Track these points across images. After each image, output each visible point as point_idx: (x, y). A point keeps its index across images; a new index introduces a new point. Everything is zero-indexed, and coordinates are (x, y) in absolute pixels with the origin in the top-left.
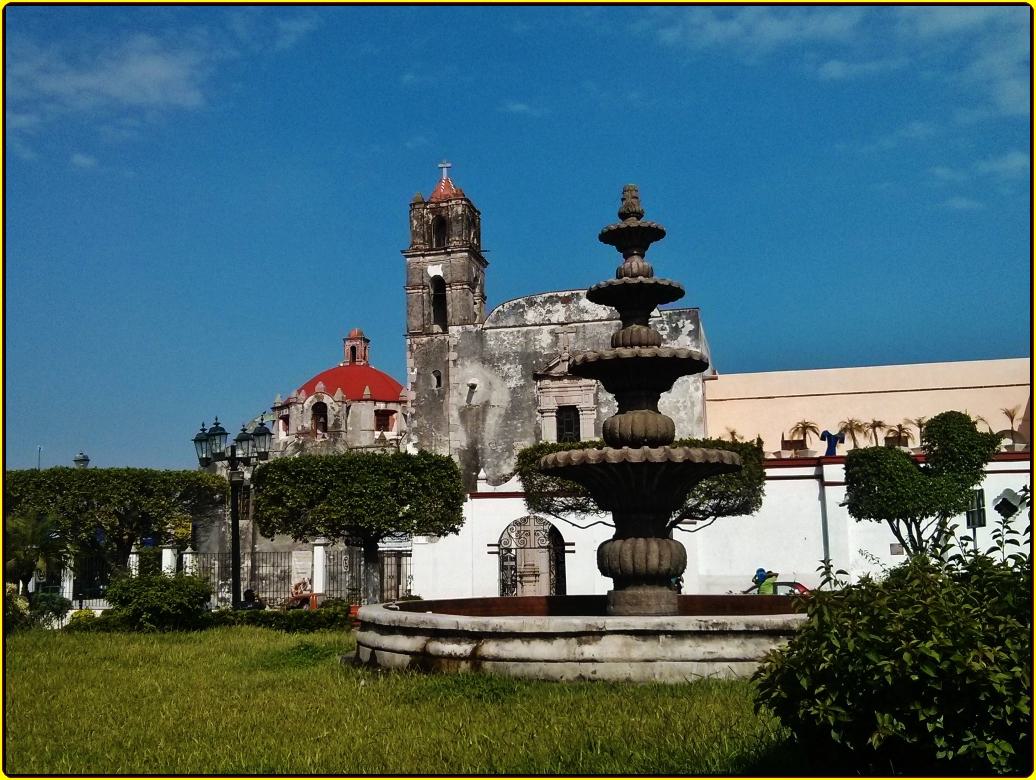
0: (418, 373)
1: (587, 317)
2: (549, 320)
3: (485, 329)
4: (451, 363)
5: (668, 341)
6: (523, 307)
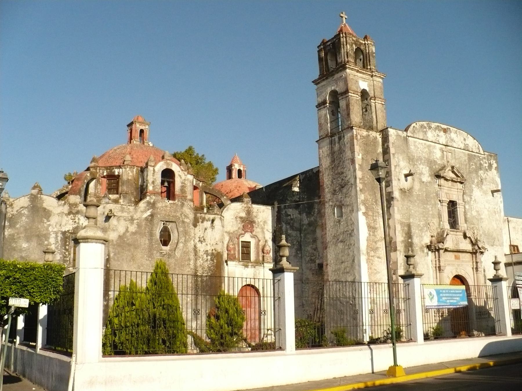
0: (362, 158)
1: (455, 145)
2: (438, 141)
3: (409, 137)
4: (391, 155)
5: (488, 171)
6: (425, 128)
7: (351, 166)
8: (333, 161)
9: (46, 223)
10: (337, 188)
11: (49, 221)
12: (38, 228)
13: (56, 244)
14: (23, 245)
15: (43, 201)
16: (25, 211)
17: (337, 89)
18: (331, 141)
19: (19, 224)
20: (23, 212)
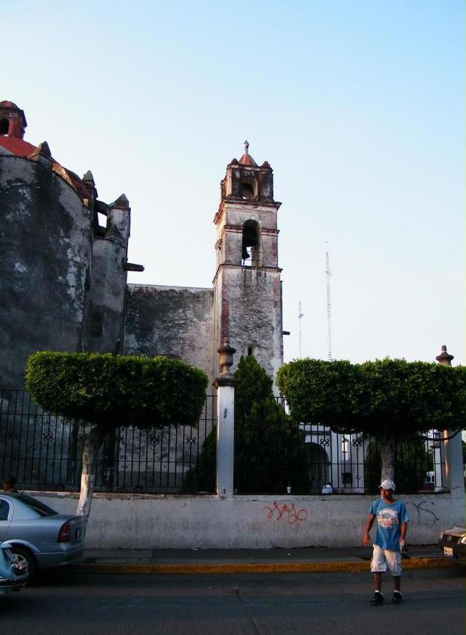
7: (274, 310)
8: (246, 295)
9: (62, 237)
10: (250, 326)
11: (69, 238)
12: (48, 243)
13: (77, 289)
14: (17, 265)
15: (60, 190)
16: (25, 191)
17: (260, 222)
18: (245, 272)
19: (12, 214)
20: (20, 191)
